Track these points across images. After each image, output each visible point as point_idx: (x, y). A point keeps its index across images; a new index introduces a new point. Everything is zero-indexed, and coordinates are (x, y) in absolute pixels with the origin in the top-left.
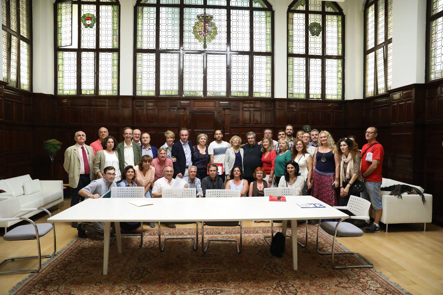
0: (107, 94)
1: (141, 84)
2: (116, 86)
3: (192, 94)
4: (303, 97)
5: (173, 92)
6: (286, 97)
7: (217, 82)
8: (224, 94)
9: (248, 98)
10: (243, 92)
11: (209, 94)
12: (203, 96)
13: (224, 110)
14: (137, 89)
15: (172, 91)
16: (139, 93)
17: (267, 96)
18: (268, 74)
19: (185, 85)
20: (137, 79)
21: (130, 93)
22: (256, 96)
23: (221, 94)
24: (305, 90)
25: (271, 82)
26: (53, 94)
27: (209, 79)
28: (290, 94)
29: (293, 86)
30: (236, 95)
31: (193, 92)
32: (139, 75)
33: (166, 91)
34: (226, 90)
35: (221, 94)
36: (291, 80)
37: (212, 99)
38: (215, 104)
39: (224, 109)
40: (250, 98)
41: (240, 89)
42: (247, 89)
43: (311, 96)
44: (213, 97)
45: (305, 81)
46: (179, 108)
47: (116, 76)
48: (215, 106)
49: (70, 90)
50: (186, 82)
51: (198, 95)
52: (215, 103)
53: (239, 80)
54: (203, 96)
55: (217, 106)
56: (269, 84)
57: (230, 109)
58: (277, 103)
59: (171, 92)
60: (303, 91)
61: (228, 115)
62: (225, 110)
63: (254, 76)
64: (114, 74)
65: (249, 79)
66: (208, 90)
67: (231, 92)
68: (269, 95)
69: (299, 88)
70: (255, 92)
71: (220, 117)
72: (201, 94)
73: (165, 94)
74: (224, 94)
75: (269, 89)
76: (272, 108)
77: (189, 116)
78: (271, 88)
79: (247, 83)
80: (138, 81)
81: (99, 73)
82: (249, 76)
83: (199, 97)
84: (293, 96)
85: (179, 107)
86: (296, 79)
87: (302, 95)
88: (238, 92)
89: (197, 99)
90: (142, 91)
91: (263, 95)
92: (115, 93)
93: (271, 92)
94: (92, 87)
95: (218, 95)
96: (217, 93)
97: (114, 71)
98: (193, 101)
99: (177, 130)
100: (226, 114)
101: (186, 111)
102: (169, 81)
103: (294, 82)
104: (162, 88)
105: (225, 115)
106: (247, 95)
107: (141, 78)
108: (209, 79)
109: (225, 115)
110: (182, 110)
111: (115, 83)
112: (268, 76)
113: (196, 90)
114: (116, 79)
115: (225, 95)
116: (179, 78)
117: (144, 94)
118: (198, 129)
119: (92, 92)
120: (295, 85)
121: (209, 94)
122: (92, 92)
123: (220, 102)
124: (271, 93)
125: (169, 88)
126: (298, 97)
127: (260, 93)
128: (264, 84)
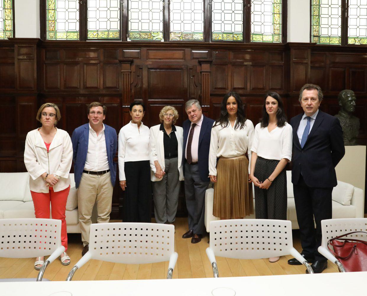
1: (55, 20)
2: (9, 23)
3: (144, 37)
4: (336, 42)
5: (111, 33)
6: (308, 42)
7: (187, 17)
8: (200, 37)
9: (243, 44)
10: (232, 33)
11: (173, 37)
12: (163, 41)
13: (201, 65)
14: (47, 29)
15: (108, 31)
16: (50, 36)
17: (275, 40)
18: (275, 1)
20: (47, 11)
21: (33, 33)
22: (255, 40)
23: (195, 36)
24: (340, 29)
25: (281, 16)
27: (174, 11)
28: (314, 36)
29: (319, 23)
30: (220, 38)
31: (146, 33)
33: (97, 31)
34: (203, 30)
35: (195, 36)
36: (316, 13)
37: (178, 45)
38: (184, 54)
39: (200, 63)
40: (245, 43)
41: (228, 29)
42: (239, 28)
43: (350, 42)
44: (182, 41)
45: (340, 14)
46: (121, 62)
47: (9, 6)
48: (184, 58)
50: (133, 16)
51: (154, 39)
52: (185, 53)
53: (225, 12)
54: (163, 41)
55: (188, 57)
56: (279, 19)
57: (210, 62)
58: (293, 52)
59: (106, 33)
60: (337, 32)
61: (207, 73)
62: (202, 65)
63: (252, 4)
65: (244, 11)
66: (171, 30)
67: (212, 33)
68: (278, 39)
69: (329, 26)
70: (254, 34)
71: (193, 76)
72: (159, 37)
73: (96, 36)
74: (200, 37)
75: (279, 27)
76: (283, 62)
77: (138, 76)
78: (281, 26)
79: (240, 17)
80: (50, 15)
82: (244, 6)
83: (157, 41)
84: (319, 41)
85: (121, 59)
86: (324, 11)
87: (334, 40)
88: (224, 33)
89: (152, 44)
90: (55, 32)
91: (268, 39)
92: (9, 35)
93: (281, 33)
95: (189, 38)
96: (187, 35)
98: (147, 48)
99: (119, 100)
100: (203, 72)
101: (133, 67)
102: (103, 14)
103: (322, 16)
104: (91, 26)
105: (201, 72)
106: (240, 38)
108: (174, 11)
109: (202, 73)
110: (127, 66)
111: (9, 18)
112: (276, 6)
114: (9, 10)
115: (202, 38)
116: (120, 9)
117: (61, 36)
118: (154, 99)
120: (324, 21)
121: (173, 37)
123: (193, 51)
124: (281, 36)
125: (103, 26)
126: (328, 42)
127: (262, 34)
128: (269, 19)
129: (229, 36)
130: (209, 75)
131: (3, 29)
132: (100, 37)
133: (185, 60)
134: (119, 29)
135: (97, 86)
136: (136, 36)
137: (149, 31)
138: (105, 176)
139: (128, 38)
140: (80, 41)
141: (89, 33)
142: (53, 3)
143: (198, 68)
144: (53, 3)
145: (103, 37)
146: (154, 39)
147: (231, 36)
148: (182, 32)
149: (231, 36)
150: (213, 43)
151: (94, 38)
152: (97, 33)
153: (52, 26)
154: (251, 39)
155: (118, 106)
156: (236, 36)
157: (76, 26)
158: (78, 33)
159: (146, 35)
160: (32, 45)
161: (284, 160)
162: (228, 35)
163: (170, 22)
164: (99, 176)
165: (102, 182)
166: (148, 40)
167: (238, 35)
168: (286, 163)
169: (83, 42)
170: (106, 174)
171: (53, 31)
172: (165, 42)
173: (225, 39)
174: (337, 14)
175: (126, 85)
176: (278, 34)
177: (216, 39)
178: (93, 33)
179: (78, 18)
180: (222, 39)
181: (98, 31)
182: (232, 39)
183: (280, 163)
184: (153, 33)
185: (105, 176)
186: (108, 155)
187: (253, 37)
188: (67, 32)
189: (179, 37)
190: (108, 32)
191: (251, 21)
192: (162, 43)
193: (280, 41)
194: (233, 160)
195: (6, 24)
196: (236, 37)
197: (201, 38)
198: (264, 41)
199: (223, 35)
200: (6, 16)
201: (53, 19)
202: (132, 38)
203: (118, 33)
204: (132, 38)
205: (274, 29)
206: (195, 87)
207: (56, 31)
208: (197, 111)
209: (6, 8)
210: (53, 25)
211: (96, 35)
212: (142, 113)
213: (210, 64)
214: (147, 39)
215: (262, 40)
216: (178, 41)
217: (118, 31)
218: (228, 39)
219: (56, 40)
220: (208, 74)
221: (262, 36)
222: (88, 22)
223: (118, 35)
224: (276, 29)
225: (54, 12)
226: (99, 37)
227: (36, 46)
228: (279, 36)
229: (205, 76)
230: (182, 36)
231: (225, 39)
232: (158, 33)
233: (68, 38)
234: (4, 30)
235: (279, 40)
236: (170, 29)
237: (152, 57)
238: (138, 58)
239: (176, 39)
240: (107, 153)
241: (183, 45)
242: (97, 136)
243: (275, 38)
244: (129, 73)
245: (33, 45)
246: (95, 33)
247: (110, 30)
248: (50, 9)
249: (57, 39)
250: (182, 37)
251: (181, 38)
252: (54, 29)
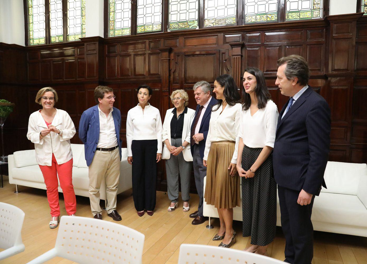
0: (76, 39)
1: (114, 21)
3: (182, 26)
5: (154, 26)
10: (266, 14)
12: (198, 28)
15: (153, 24)
16: (111, 34)
17: (314, 16)
19: (171, 13)
22: (291, 18)
26: (23, 44)
30: (253, 20)
32: (111, 8)
33: (144, 25)
35: (228, 21)
37: (211, 31)
48: (217, 43)
49: (39, 39)
51: (190, 27)
54: (198, 28)
55: (221, 42)
59: (151, 27)
61: (238, 57)
64: (83, 10)
66: (206, 17)
70: (289, 12)
71: (226, 60)
73: (143, 30)
81: (67, 11)
88: (257, 14)
90: (114, 30)
94: (61, 32)
97: (83, 6)
101: (172, 55)
104: (140, 21)
107: (113, 11)
113: (187, 19)
115: (235, 21)
117: (118, 34)
119: (61, 39)
121: (208, 24)
122: (61, 39)
123: (226, 36)
124: (321, 11)
125: (149, 20)
129: (262, 17)
131: (81, 32)
132: (147, 30)
133: (218, 45)
134: (161, 22)
135: (144, 73)
136: (175, 26)
137: (186, 20)
138: (115, 152)
139: (168, 29)
140: (131, 36)
141: (138, 28)
142: (113, 6)
144: (113, 6)
145: (149, 30)
146: (190, 28)
147: (265, 17)
148: (215, 19)
149: (265, 17)
150: (246, 25)
151: (142, 32)
152: (144, 27)
153: (112, 25)
154: (286, 17)
155: (159, 90)
156: (270, 16)
157: (128, 23)
158: (130, 29)
159: (184, 24)
160: (95, 43)
161: (266, 147)
162: (262, 16)
163: (205, 9)
164: (110, 152)
165: (113, 157)
166: (185, 29)
167: (272, 15)
168: (269, 151)
169: (134, 36)
170: (115, 150)
171: (113, 29)
172: (200, 29)
173: (258, 21)
174: (77, 15)
175: (165, 72)
176: (318, 9)
177: (249, 21)
178: (141, 27)
179: (130, 16)
180: (255, 21)
181: (145, 25)
182: (266, 20)
183: (263, 149)
184: (190, 22)
185: (115, 152)
186: (116, 133)
187: (289, 15)
188: (123, 29)
189: (213, 23)
190: (153, 25)
191: (205, 7)
192: (197, 30)
193: (320, 17)
194: (216, 144)
195: (83, 28)
196: (270, 17)
197: (234, 22)
198: (301, 18)
199: (256, 17)
200: (83, 22)
201: (113, 20)
202: (172, 28)
203: (160, 25)
204: (172, 28)
205: (314, 4)
206: (228, 71)
207: (115, 29)
208: (202, 94)
209: (83, 15)
210: (112, 25)
211: (143, 30)
212: (147, 96)
214: (184, 28)
215: (298, 18)
216: (212, 27)
217: (160, 24)
218: (261, 20)
219: (115, 37)
220: (239, 58)
221: (299, 13)
222: (137, 18)
223: (160, 27)
224: (316, 3)
225: (114, 14)
226: (145, 31)
227: (98, 42)
228: (320, 11)
229: (235, 59)
230: (215, 22)
231: (259, 21)
232: (193, 21)
233: (123, 34)
234: (81, 33)
235: (319, 15)
236: (204, 17)
237: (188, 45)
239: (210, 25)
240: (116, 131)
241: (216, 30)
242: (106, 118)
243: (314, 13)
245: (96, 43)
246: (143, 28)
247: (146, 24)
248: (111, 12)
249: (115, 36)
250: (216, 23)
251: (215, 24)
252: (113, 28)
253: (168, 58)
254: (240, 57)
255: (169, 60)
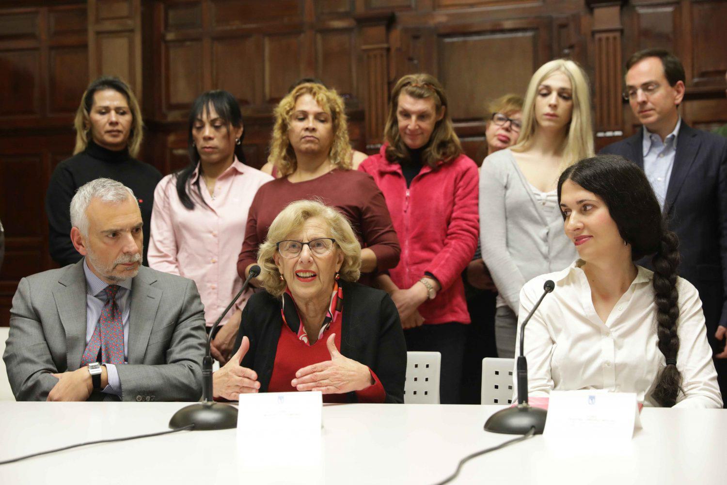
61: (611, 35)
101: (396, 34)
110: (378, 31)
130: (618, 38)
143: (585, 20)
213: (622, 7)
220: (615, 38)
238: (408, 8)
244: (384, 53)
253: (385, 46)
254: (618, 34)
255: (388, 50)
